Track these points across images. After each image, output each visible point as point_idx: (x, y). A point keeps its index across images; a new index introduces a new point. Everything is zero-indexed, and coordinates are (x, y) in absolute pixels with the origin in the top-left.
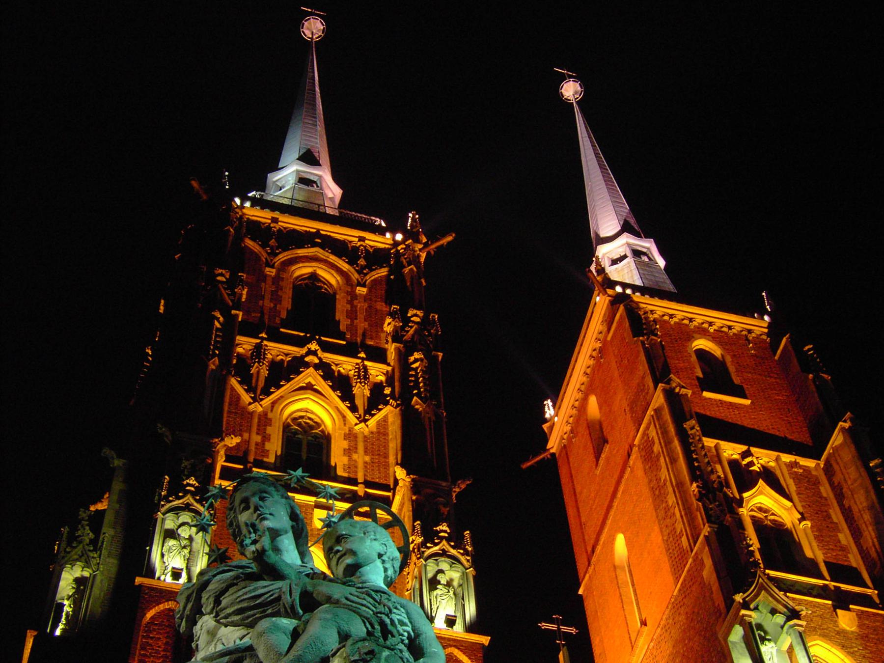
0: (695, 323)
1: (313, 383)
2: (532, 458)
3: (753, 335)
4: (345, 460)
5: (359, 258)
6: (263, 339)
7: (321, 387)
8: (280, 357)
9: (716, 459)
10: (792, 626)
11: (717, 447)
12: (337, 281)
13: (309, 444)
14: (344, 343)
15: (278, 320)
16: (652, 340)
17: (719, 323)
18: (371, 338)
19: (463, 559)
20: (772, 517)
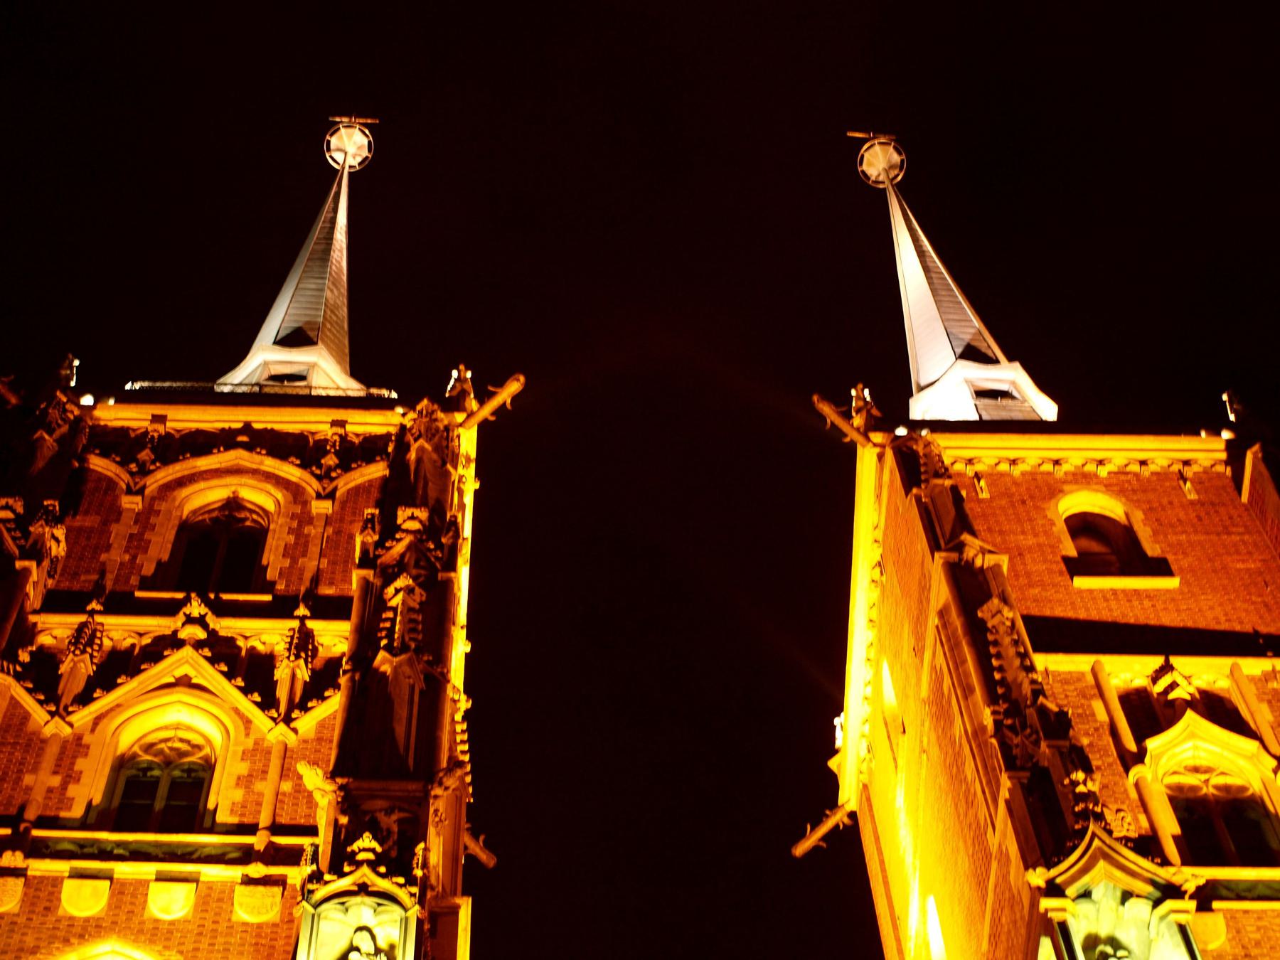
0: (1066, 467)
1: (192, 673)
2: (812, 830)
3: (1195, 468)
4: (238, 795)
5: (327, 453)
6: (92, 613)
7: (206, 679)
8: (129, 641)
9: (1096, 691)
10: (1163, 918)
11: (1094, 672)
12: (278, 502)
13: (174, 784)
14: (268, 598)
15: (134, 580)
16: (936, 486)
17: (1118, 460)
18: (331, 584)
19: (402, 894)
20: (1221, 780)
